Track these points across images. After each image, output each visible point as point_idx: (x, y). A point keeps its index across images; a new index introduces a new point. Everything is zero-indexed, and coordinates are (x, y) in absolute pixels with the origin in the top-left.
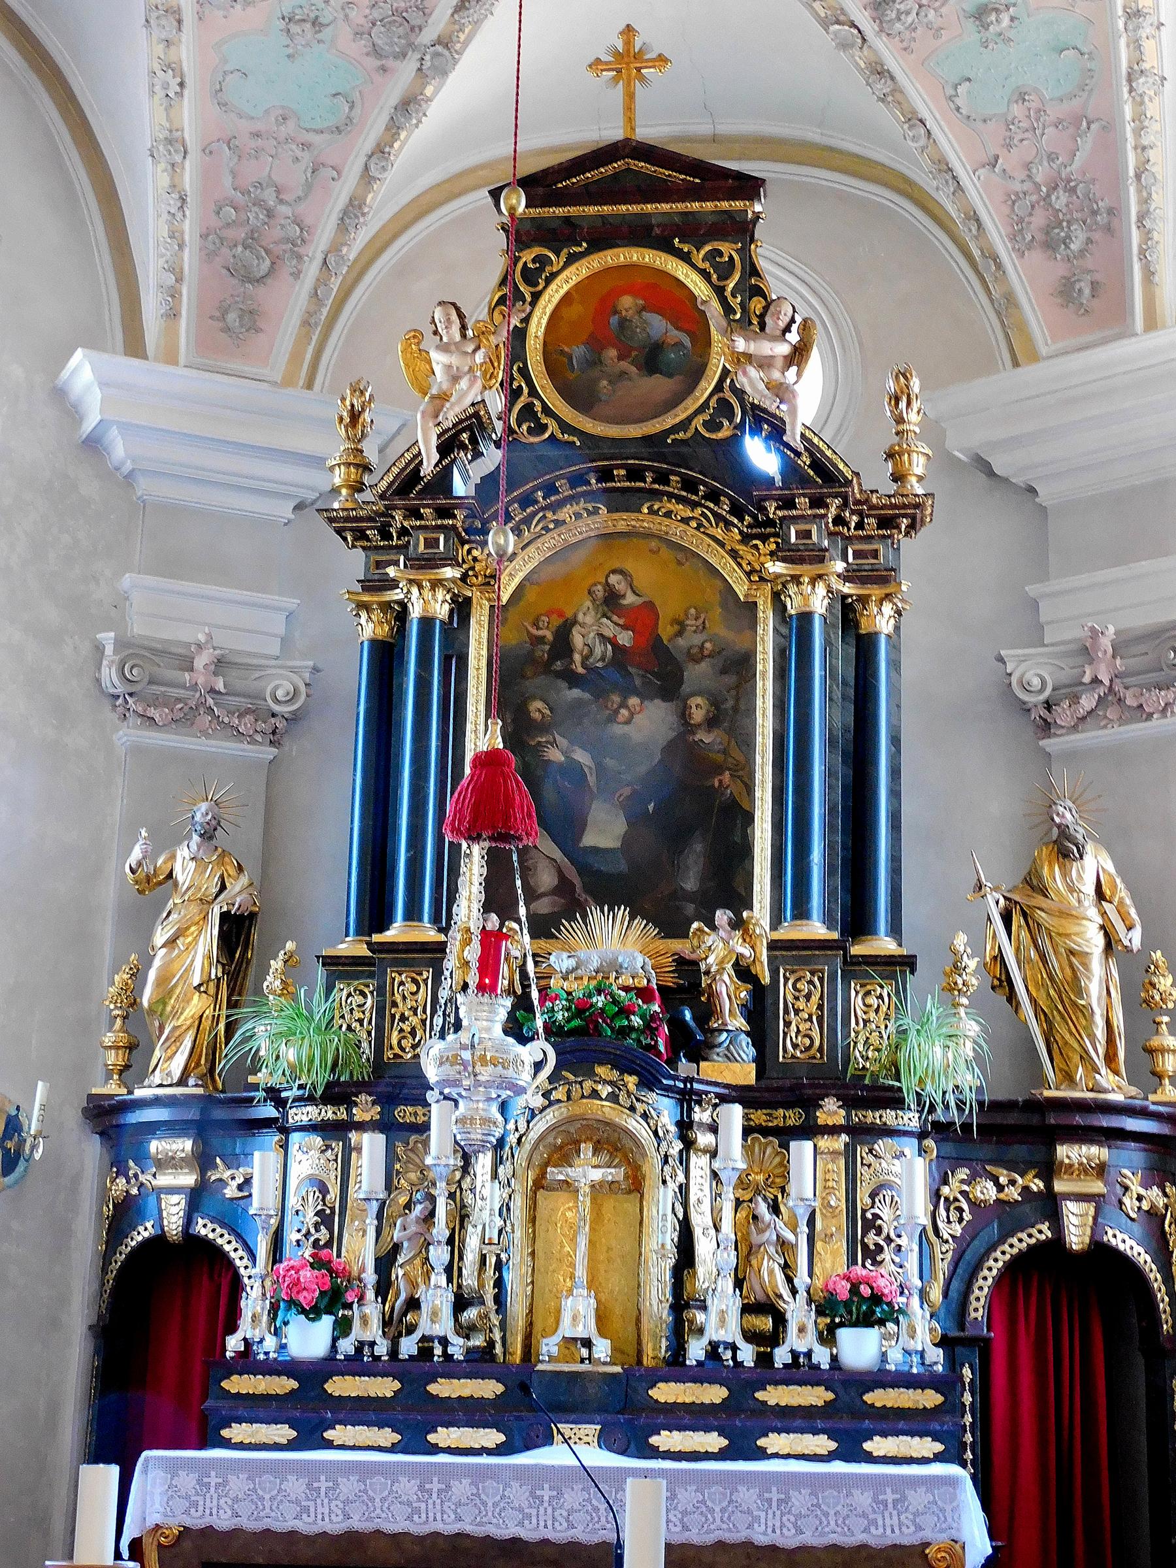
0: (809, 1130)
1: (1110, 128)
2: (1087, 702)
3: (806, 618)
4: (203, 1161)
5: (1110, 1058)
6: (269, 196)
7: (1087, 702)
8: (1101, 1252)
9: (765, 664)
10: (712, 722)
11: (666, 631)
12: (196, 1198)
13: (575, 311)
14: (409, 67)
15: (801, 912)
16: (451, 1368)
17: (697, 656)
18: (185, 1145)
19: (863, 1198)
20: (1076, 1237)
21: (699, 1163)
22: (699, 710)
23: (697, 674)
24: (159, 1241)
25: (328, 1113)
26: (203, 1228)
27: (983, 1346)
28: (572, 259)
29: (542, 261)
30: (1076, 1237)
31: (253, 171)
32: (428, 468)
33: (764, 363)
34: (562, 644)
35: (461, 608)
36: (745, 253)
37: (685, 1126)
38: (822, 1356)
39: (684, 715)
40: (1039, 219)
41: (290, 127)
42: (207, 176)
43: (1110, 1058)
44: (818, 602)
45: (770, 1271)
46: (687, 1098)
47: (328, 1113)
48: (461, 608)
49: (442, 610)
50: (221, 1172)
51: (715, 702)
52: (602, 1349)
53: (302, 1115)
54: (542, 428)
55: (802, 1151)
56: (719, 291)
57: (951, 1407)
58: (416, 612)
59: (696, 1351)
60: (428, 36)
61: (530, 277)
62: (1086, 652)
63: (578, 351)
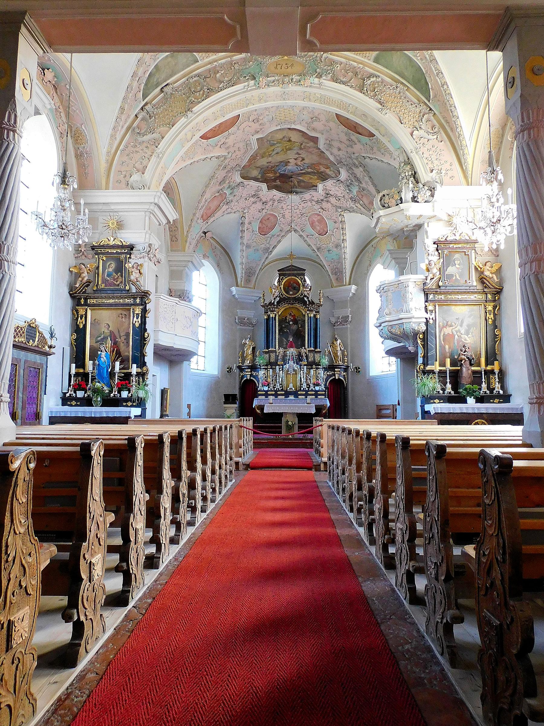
0: (312, 368)
1: (342, 263)
2: (339, 323)
3: (311, 317)
4: (251, 372)
5: (340, 360)
6: (252, 268)
7: (339, 323)
8: (339, 379)
9: (306, 321)
10: (301, 327)
11: (296, 318)
12: (251, 375)
13: (285, 283)
14: (267, 254)
15: (311, 347)
16: (279, 391)
17: (300, 320)
18: (249, 370)
19: (317, 374)
20: (337, 378)
21: (302, 371)
22: (300, 326)
23: (299, 322)
24: (247, 379)
25: (266, 367)
26: (252, 378)
27: (328, 388)
28: (286, 278)
29: (283, 278)
30: (337, 378)
31: (250, 265)
32: (272, 302)
33: (307, 291)
34: (286, 319)
35: (276, 315)
36: (304, 277)
37: (300, 368)
38: (314, 389)
39: (298, 326)
40: (334, 272)
41: (254, 261)
42: (245, 267)
43: (340, 360)
44: (312, 316)
45: (309, 381)
46: (301, 365)
47: (266, 367)
48: (276, 315)
49: (274, 316)
50: (253, 372)
51: (301, 325)
52: (293, 389)
53: (262, 367)
54: (283, 296)
55: (312, 371)
56: (301, 281)
57: (325, 393)
58: (271, 316)
59: (302, 389)
60: (269, 251)
61: (282, 279)
62: (338, 318)
63: (287, 288)
